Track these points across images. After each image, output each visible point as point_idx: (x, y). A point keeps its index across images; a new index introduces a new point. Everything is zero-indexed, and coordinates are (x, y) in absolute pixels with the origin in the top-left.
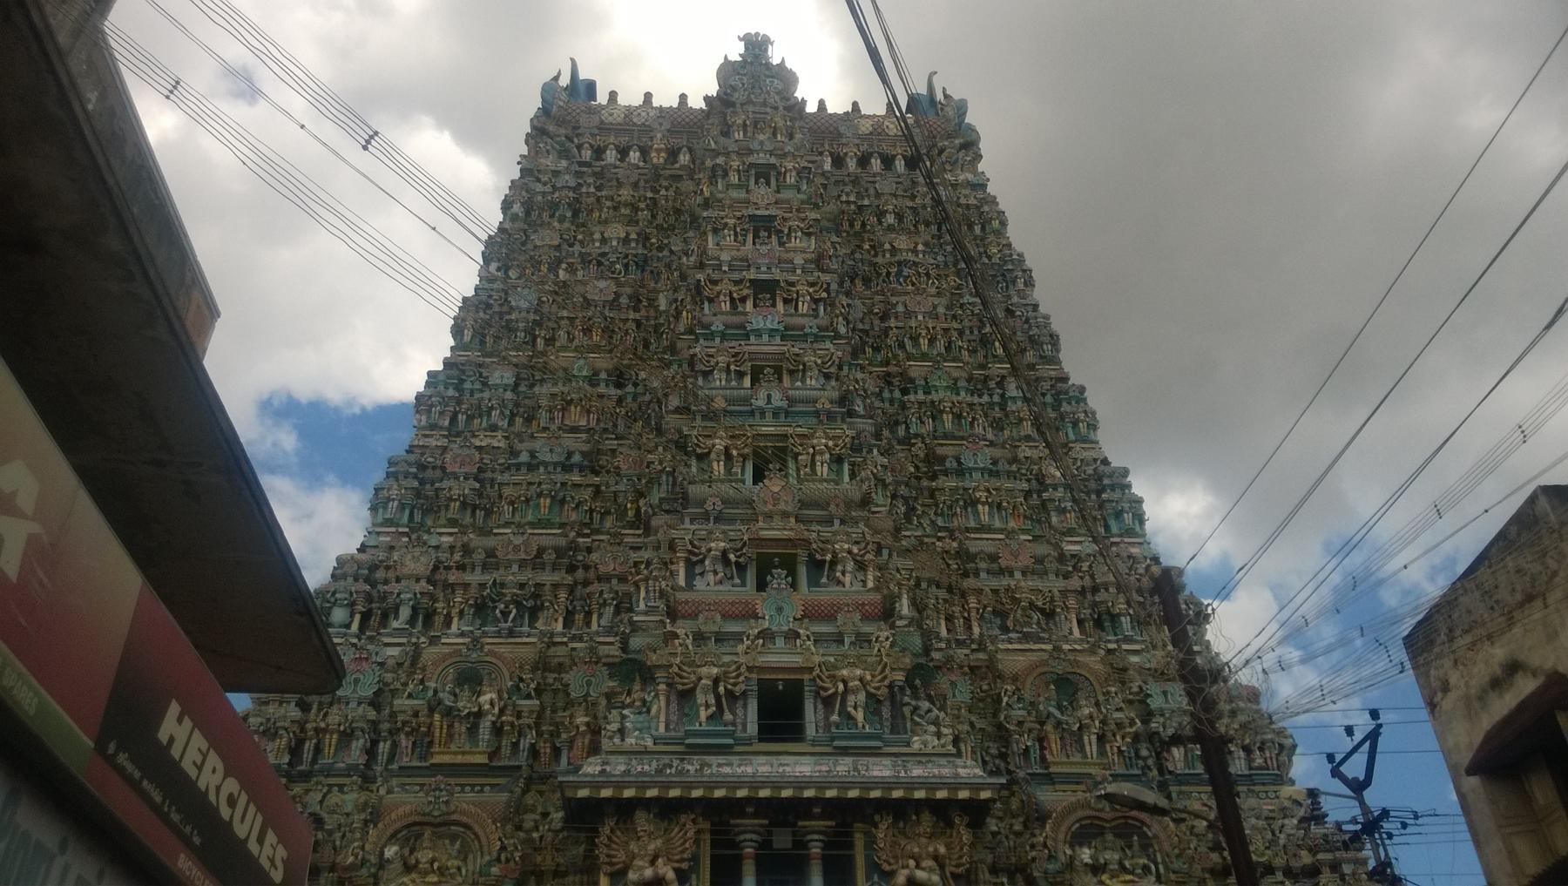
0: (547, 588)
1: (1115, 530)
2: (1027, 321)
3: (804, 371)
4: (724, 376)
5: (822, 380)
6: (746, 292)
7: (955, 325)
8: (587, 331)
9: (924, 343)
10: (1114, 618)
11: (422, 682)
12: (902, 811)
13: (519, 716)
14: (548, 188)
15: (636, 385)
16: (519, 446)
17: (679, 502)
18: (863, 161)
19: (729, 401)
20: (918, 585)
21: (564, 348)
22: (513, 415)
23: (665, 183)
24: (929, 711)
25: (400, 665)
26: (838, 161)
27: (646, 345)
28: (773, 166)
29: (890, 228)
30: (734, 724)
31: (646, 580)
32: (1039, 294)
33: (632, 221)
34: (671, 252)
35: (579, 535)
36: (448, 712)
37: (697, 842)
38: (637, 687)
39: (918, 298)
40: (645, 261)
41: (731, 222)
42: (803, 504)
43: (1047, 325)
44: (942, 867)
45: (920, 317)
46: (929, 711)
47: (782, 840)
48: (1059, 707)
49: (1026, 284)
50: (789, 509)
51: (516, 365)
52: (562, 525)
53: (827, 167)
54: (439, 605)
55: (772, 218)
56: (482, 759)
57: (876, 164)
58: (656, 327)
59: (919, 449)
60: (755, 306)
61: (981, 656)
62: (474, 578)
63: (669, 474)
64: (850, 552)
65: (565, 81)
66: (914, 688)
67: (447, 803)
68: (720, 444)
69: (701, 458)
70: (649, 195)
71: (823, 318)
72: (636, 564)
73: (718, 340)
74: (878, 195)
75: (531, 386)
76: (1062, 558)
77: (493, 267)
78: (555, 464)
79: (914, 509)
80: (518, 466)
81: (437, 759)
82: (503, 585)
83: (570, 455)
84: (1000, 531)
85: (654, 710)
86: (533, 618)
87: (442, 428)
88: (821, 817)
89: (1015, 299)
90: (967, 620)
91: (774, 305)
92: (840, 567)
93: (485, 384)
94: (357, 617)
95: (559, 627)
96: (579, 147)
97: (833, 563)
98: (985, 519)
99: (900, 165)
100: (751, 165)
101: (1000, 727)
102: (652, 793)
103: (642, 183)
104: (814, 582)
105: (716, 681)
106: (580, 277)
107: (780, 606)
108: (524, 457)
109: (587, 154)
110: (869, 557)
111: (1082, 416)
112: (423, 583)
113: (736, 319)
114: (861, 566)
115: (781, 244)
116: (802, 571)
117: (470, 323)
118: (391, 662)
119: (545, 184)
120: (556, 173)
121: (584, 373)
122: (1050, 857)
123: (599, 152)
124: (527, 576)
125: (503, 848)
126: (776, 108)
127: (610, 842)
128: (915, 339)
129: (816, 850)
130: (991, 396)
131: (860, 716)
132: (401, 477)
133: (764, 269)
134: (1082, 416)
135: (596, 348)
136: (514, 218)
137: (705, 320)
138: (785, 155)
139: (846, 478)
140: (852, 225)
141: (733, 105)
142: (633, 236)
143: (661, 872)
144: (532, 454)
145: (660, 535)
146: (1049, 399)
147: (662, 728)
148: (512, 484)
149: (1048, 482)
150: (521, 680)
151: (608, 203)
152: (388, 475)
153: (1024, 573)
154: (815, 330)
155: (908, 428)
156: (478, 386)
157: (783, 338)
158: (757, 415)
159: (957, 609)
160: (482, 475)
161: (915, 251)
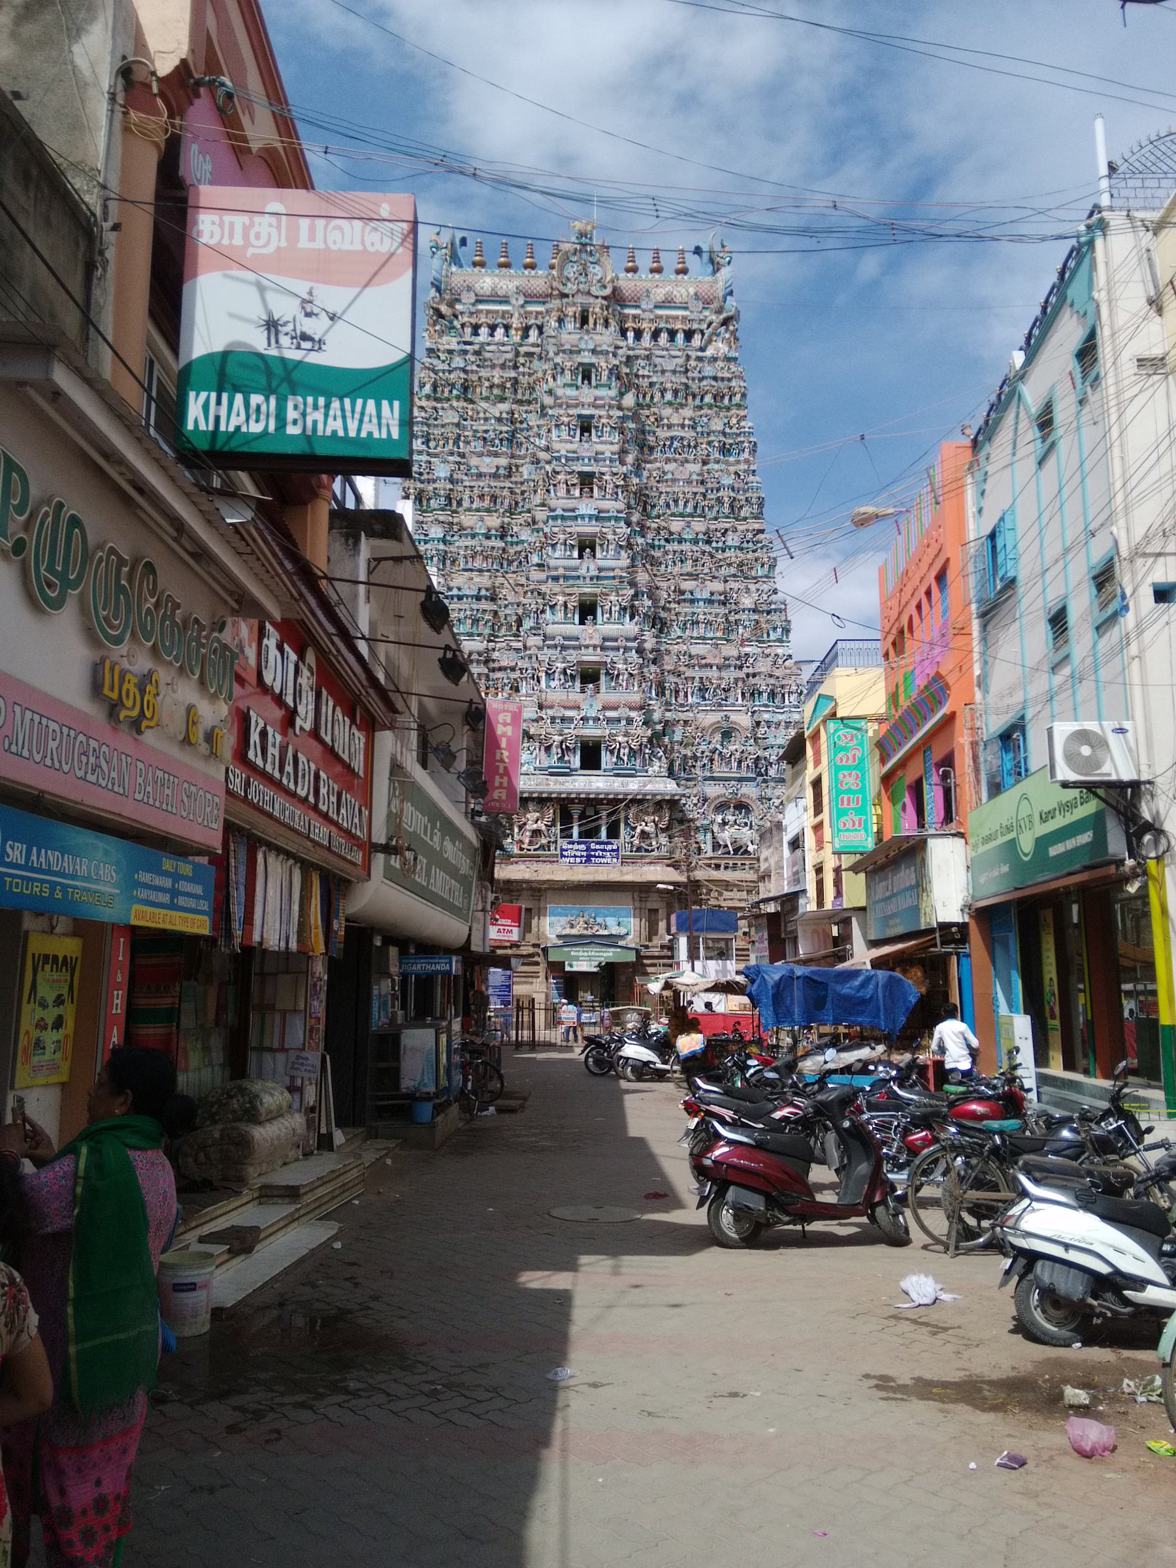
1: (772, 637)
6: (575, 481)
8: (482, 497)
9: (681, 503)
10: (760, 693)
15: (512, 536)
16: (452, 584)
18: (656, 335)
21: (469, 510)
28: (593, 365)
29: (670, 404)
35: (489, 641)
42: (605, 639)
50: (597, 642)
55: (592, 417)
57: (664, 336)
68: (561, 599)
78: (472, 597)
90: (686, 693)
97: (618, 676)
99: (680, 337)
100: (580, 364)
109: (468, 330)
113: (570, 504)
116: (603, 678)
120: (450, 352)
123: (476, 329)
128: (676, 501)
131: (625, 758)
133: (586, 461)
156: (422, 537)
161: (683, 426)
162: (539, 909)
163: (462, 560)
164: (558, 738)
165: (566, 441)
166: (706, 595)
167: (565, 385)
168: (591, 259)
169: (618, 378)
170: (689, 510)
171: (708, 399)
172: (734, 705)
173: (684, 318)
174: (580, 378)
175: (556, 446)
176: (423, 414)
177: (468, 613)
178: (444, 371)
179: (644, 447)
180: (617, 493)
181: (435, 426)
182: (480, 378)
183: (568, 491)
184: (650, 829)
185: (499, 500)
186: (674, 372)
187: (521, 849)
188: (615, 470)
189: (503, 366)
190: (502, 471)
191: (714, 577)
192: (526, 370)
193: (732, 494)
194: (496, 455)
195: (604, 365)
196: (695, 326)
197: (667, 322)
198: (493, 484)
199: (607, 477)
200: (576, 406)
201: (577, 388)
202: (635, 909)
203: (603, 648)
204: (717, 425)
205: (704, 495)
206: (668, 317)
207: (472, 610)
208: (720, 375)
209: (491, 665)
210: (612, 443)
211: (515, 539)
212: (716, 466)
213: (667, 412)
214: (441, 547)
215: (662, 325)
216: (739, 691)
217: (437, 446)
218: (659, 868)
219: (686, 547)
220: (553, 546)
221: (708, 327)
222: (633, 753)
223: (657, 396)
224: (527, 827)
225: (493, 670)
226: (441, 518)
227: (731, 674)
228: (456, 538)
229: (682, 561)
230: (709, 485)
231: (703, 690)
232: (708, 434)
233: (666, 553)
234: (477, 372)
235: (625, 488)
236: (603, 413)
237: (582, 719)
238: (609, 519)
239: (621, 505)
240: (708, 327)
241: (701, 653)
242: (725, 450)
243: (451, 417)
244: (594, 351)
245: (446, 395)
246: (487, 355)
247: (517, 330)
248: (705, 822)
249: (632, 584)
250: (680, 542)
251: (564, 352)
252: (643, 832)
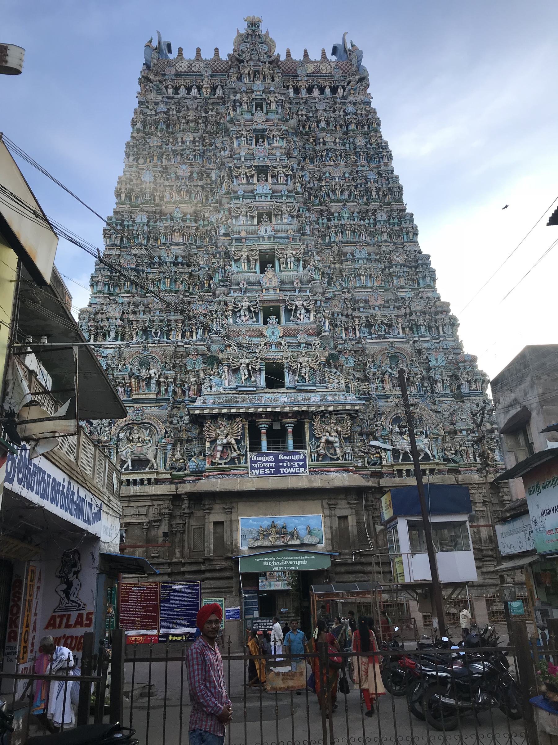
0: (173, 321)
2: (388, 179)
3: (282, 215)
4: (245, 219)
5: (290, 219)
6: (253, 172)
7: (353, 183)
9: (338, 193)
10: (418, 327)
11: (124, 365)
12: (323, 415)
13: (167, 379)
14: (153, 113)
15: (204, 220)
17: (227, 282)
18: (310, 90)
19: (248, 232)
20: (333, 315)
22: (148, 238)
23: (211, 107)
24: (336, 372)
25: (114, 357)
26: (297, 90)
27: (207, 199)
29: (323, 130)
30: (256, 381)
31: (216, 318)
32: (394, 164)
33: (196, 130)
34: (216, 146)
36: (137, 378)
38: (215, 367)
39: (336, 169)
40: (204, 153)
41: (245, 133)
42: (282, 283)
43: (397, 181)
44: (339, 435)
45: (337, 180)
46: (336, 372)
47: (277, 427)
48: (391, 368)
49: (388, 160)
50: (276, 285)
51: (147, 212)
52: (176, 292)
53: (292, 95)
54: (127, 330)
55: (265, 130)
56: (154, 396)
58: (212, 189)
59: (335, 249)
60: (258, 181)
61: (360, 346)
62: (141, 317)
63: (222, 268)
64: (303, 305)
65: (155, 44)
66: (329, 364)
67: (142, 415)
68: (245, 254)
69: (236, 261)
70: (203, 115)
71: (290, 186)
72: (211, 312)
73: (241, 199)
74: (317, 110)
75: (156, 222)
76: (397, 300)
77: (131, 158)
78: (171, 263)
79: (332, 278)
81: (135, 397)
82: (153, 321)
83: (177, 257)
84: (371, 288)
85: (223, 376)
86: (168, 336)
87: (116, 246)
88: (291, 418)
89: (383, 168)
90: (354, 329)
91: (267, 180)
92: (298, 312)
93: (134, 222)
94: (92, 336)
95: (179, 338)
96: (166, 87)
97: (296, 310)
98: (364, 282)
99: (328, 91)
101: (366, 376)
102: (225, 411)
103: (199, 108)
104: (288, 320)
105: (248, 365)
106: (173, 163)
107: (274, 331)
109: (171, 90)
110: (311, 307)
111: (411, 229)
112: (119, 320)
113: (250, 188)
114: (308, 311)
115: (270, 144)
116: (282, 313)
117: (123, 190)
118: (110, 356)
119: (151, 110)
120: (156, 104)
121: (180, 216)
122: (383, 429)
123: (176, 89)
124: (164, 316)
125: (166, 432)
126: (265, 63)
127: (210, 431)
128: (334, 192)
129: (290, 430)
130: (369, 220)
132: (102, 271)
133: (261, 159)
134: (411, 229)
135: (184, 202)
136: (138, 131)
137: (235, 189)
138: (270, 92)
139: (302, 269)
140: (304, 128)
141: (242, 61)
142: (197, 139)
143: (230, 441)
144: (160, 258)
145: (220, 298)
146: (396, 220)
147: (227, 384)
149: (393, 263)
150: (166, 363)
151: (184, 121)
152: (96, 269)
153: (379, 308)
154: (286, 193)
155: (330, 238)
156: (131, 223)
157: (272, 197)
158: (261, 239)
159: (350, 325)
160: (138, 268)
161: (335, 143)
162: (231, 521)
168: (259, 40)
170: (346, 196)
171: (352, 127)
172: (397, 338)
180: (286, 181)
182: (178, 118)
183: (248, 181)
186: (325, 110)
187: (213, 463)
202: (325, 517)
216: (400, 326)
218: (345, 475)
220: (236, 217)
221: (348, 85)
223: (314, 125)
224: (218, 442)
226: (146, 209)
229: (342, 233)
237: (265, 345)
240: (348, 85)
241: (366, 298)
242: (369, 159)
247: (206, 88)
248: (384, 433)
252: (327, 441)
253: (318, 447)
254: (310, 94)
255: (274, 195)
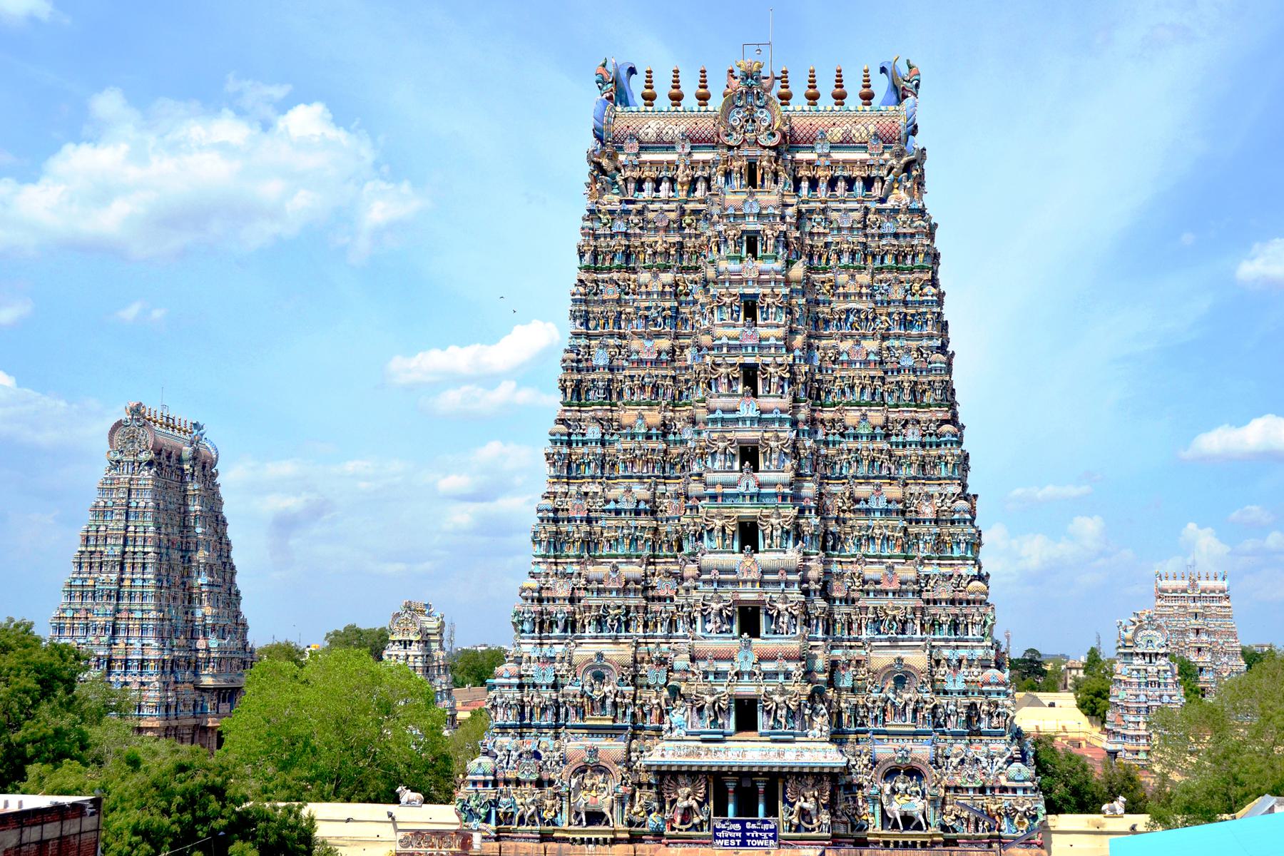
9: (857, 390)
18: (832, 183)
29: (846, 268)
37: (707, 788)
57: (841, 185)
80: (610, 511)
83: (638, 502)
97: (778, 616)
99: (859, 185)
108: (612, 506)
116: (763, 618)
128: (852, 387)
131: (783, 721)
148: (607, 526)
153: (894, 594)
163: (621, 466)
164: (709, 699)
165: (729, 326)
166: (882, 504)
167: (729, 258)
169: (787, 246)
170: (866, 397)
171: (889, 261)
173: (863, 162)
174: (745, 248)
175: (719, 331)
176: (582, 290)
177: (625, 531)
178: (605, 236)
179: (817, 323)
181: (595, 302)
184: (809, 805)
185: (661, 391)
186: (851, 229)
188: (779, 360)
189: (667, 229)
190: (664, 357)
191: (894, 479)
192: (692, 231)
193: (912, 378)
194: (658, 335)
195: (769, 232)
196: (874, 173)
197: (844, 168)
198: (654, 372)
199: (771, 369)
200: (740, 282)
201: (741, 260)
203: (763, 583)
204: (897, 293)
205: (883, 379)
206: (845, 162)
207: (629, 527)
208: (902, 230)
209: (650, 593)
210: (778, 326)
211: (678, 437)
212: (897, 343)
213: (843, 278)
214: (599, 450)
215: (838, 173)
217: (597, 325)
219: (862, 444)
222: (792, 715)
225: (653, 599)
227: (911, 602)
228: (615, 437)
230: (889, 366)
231: (877, 621)
232: (889, 303)
233: (841, 452)
234: (640, 236)
235: (792, 381)
236: (768, 291)
237: (737, 674)
238: (773, 421)
239: (786, 402)
241: (876, 577)
243: (611, 293)
244: (759, 215)
245: (607, 264)
246: (651, 216)
249: (796, 498)
250: (856, 437)
251: (728, 216)
252: (802, 809)
253: (791, 814)
254: (833, 190)
255: (761, 420)
